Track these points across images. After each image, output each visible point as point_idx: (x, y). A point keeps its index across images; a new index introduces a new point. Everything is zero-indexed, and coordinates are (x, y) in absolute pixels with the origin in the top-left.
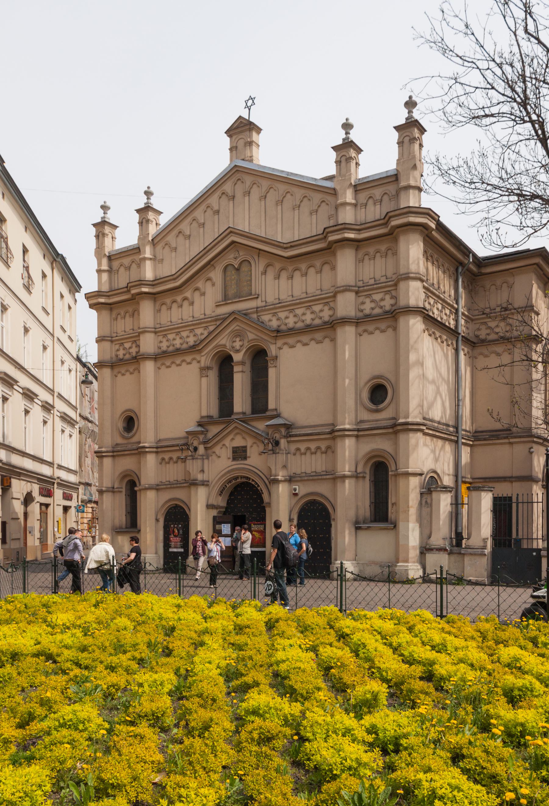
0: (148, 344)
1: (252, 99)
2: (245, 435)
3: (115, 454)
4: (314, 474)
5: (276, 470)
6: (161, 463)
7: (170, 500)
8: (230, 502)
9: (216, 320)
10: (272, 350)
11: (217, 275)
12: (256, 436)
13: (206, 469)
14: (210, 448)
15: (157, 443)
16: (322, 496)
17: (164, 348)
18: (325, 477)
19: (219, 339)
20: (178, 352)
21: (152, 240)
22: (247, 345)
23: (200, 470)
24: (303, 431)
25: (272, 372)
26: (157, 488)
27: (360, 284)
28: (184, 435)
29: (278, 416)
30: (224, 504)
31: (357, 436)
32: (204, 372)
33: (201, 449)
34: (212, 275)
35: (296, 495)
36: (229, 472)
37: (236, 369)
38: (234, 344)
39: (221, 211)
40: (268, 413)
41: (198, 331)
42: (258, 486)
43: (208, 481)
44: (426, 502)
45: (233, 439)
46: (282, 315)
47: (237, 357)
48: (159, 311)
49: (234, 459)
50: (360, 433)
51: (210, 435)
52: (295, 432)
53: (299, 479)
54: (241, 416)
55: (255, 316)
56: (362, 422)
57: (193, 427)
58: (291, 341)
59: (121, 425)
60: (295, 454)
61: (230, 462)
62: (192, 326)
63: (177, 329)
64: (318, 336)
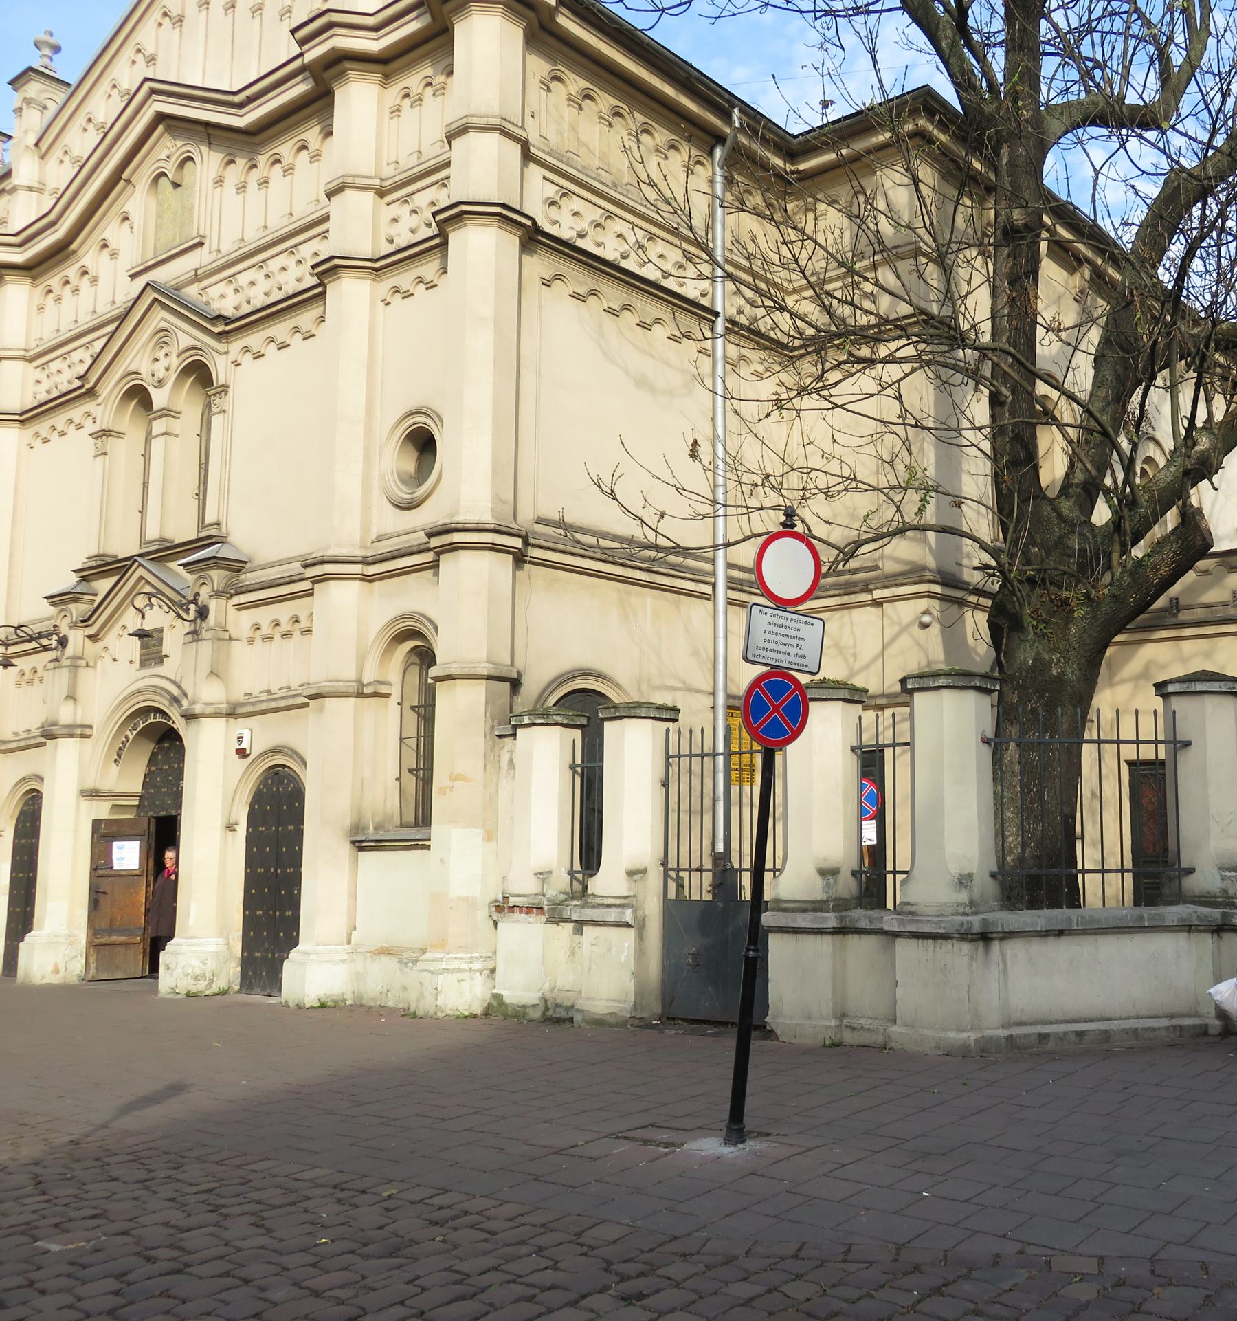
4: (284, 693)
6: (19, 685)
7: (24, 779)
13: (81, 693)
21: (37, 145)
23: (65, 694)
29: (222, 540)
35: (242, 753)
36: (125, 699)
52: (248, 578)
53: (250, 709)
56: (380, 539)
58: (254, 340)
60: (251, 641)
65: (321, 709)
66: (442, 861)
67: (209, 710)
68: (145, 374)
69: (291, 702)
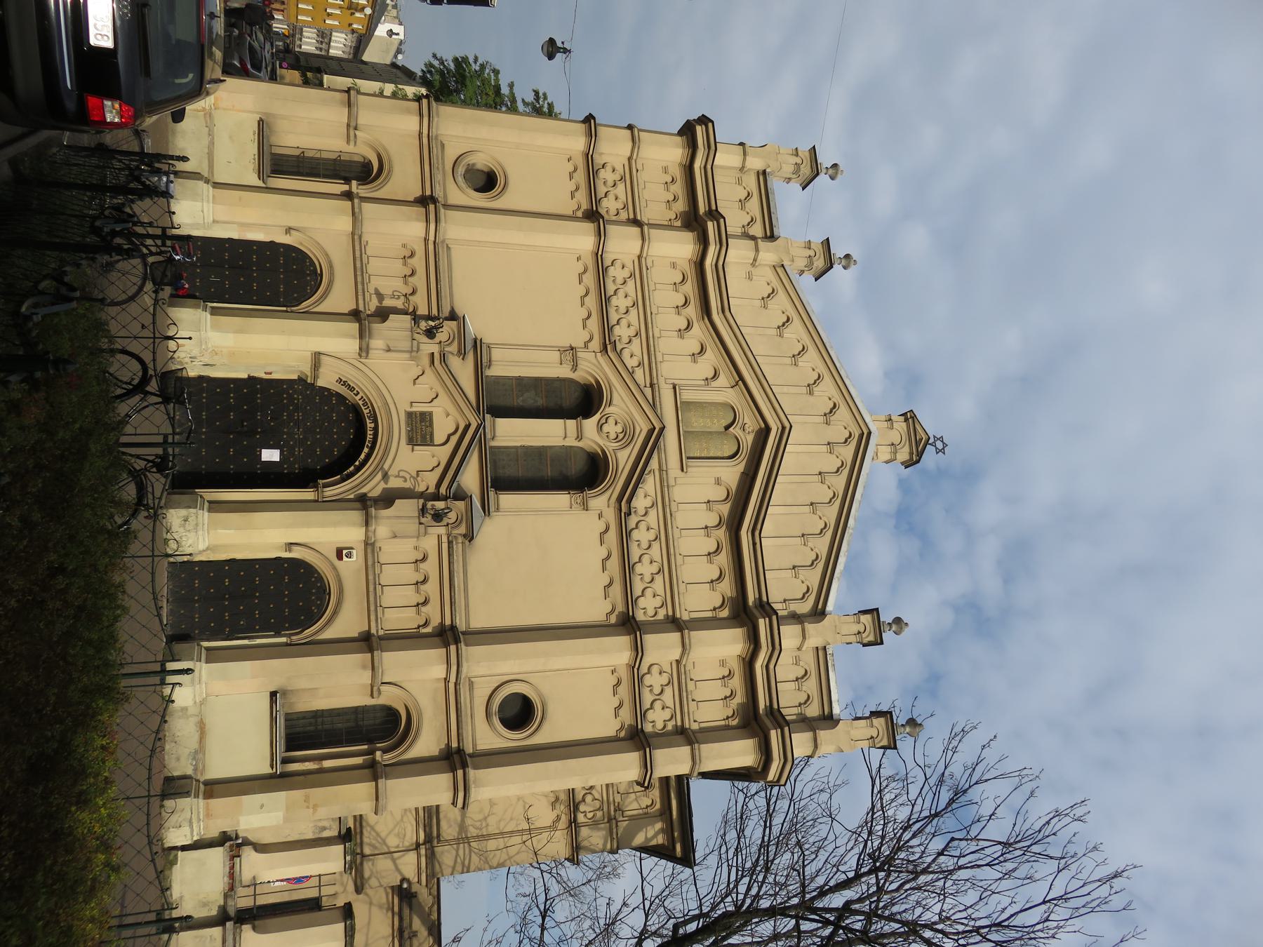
0: (622, 244)
1: (943, 451)
2: (454, 439)
3: (425, 140)
5: (389, 518)
6: (404, 246)
7: (331, 267)
8: (325, 393)
9: (652, 385)
10: (602, 501)
11: (722, 391)
12: (452, 468)
14: (433, 362)
15: (443, 241)
16: (335, 613)
17: (612, 272)
18: (373, 618)
19: (623, 395)
20: (604, 301)
22: (610, 446)
24: (458, 567)
25: (560, 500)
26: (356, 237)
27: (689, 666)
28: (460, 312)
30: (320, 383)
31: (446, 680)
32: (569, 357)
33: (430, 347)
34: (723, 380)
35: (340, 557)
37: (571, 423)
38: (611, 421)
39: (811, 399)
40: (492, 494)
41: (636, 346)
42: (358, 469)
43: (367, 357)
44: (324, 829)
45: (448, 415)
46: (652, 518)
47: (590, 424)
48: (674, 265)
49: (410, 415)
50: (454, 691)
51: (455, 362)
52: (458, 548)
53: (370, 563)
54: (489, 436)
55: (654, 464)
56: (471, 684)
57: (472, 329)
58: (612, 536)
59: (481, 161)
61: (404, 407)
62: (646, 334)
63: (642, 302)
64: (617, 589)
65: (364, 667)
66: (262, 806)
67: (370, 534)
68: (608, 410)
69: (372, 608)
